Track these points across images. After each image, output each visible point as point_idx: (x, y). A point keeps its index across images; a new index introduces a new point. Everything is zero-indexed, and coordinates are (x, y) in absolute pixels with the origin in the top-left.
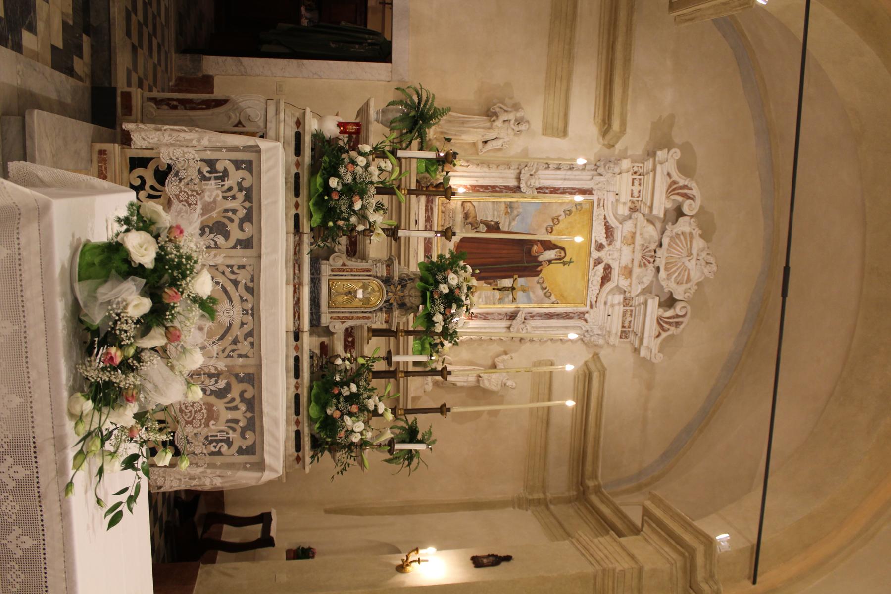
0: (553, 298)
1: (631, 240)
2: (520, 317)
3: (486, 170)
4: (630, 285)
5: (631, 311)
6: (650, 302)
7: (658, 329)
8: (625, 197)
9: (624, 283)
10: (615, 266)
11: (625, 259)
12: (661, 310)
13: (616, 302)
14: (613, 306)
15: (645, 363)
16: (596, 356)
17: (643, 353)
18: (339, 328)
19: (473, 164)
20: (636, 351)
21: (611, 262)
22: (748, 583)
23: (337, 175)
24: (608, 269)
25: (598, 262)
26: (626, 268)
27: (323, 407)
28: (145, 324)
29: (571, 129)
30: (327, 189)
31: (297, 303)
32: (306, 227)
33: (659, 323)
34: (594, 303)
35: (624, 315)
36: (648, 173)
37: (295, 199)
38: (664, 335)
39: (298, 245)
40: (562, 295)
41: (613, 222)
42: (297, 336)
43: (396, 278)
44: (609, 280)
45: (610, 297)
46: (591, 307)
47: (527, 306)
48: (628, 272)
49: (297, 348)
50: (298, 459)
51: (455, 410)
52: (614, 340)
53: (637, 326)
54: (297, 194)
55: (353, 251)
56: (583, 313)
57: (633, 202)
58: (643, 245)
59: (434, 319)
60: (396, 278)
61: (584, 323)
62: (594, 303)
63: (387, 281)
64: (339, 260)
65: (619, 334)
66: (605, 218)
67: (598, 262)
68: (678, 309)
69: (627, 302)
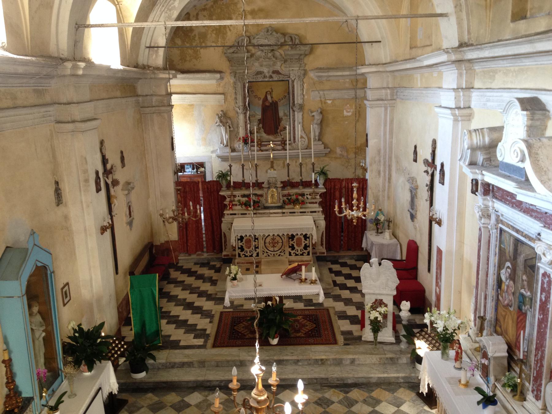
21: (271, 72)
25: (271, 77)
31: (275, 213)
39: (259, 213)
42: (284, 213)
44: (278, 71)
56: (292, 80)
63: (269, 188)
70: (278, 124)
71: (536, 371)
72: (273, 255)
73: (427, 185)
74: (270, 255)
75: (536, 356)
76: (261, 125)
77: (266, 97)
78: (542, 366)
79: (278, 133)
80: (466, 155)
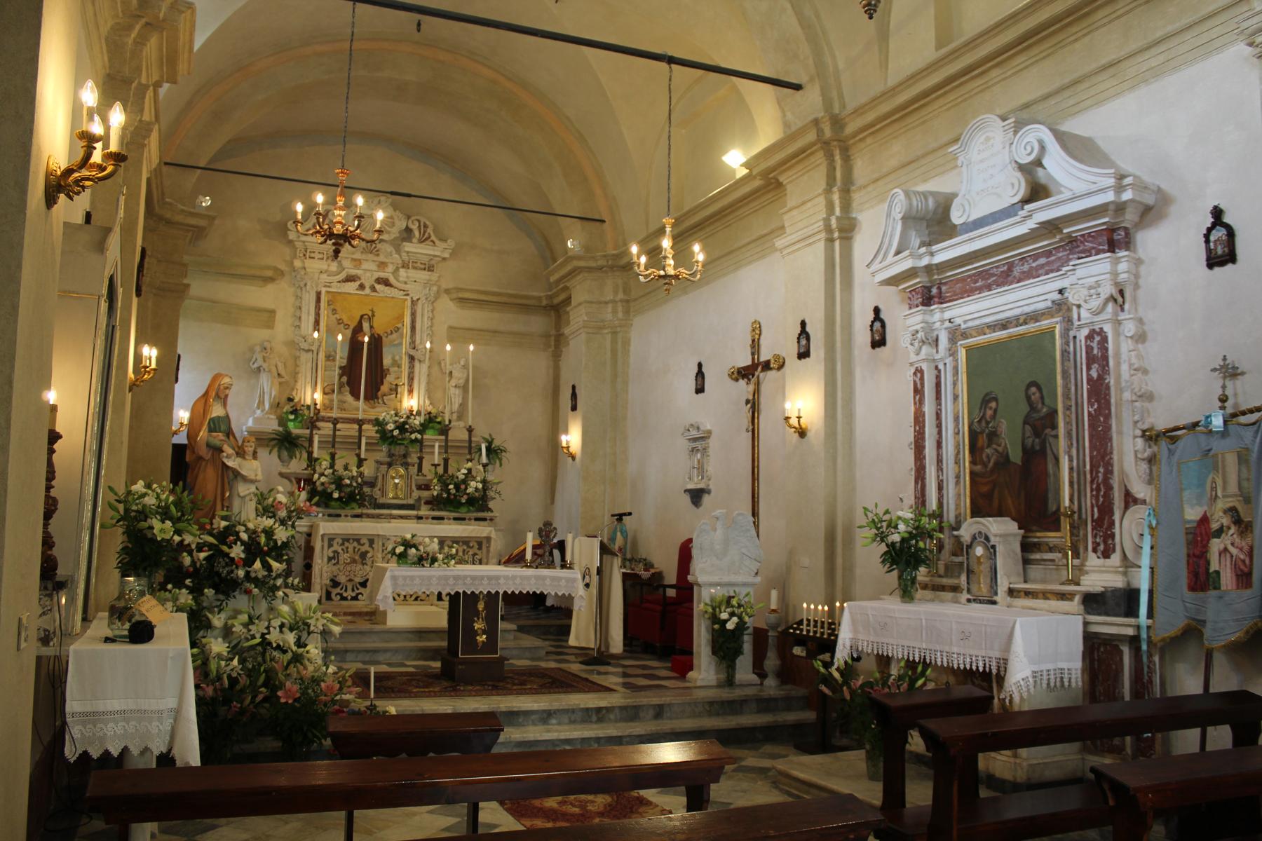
0: (400, 325)
1: (357, 263)
2: (412, 352)
3: (300, 375)
4: (392, 263)
5: (413, 262)
6: (407, 249)
7: (427, 242)
8: (323, 265)
9: (390, 268)
10: (376, 275)
11: (373, 267)
12: (415, 240)
13: (405, 274)
14: (407, 277)
15: (454, 253)
16: (447, 291)
17: (446, 255)
18: (416, 494)
19: (295, 385)
20: (444, 259)
21: (374, 278)
22: (606, 225)
23: (331, 493)
24: (379, 281)
25: (373, 289)
26: (379, 266)
27: (460, 504)
28: (417, 549)
29: (270, 306)
30: (340, 499)
31: (402, 517)
32: (359, 511)
33: (424, 241)
34: (405, 293)
35: (415, 268)
36: (305, 246)
37: (343, 517)
38: (433, 238)
39: (368, 516)
40: (398, 318)
41: (342, 276)
42: (420, 518)
43: (388, 460)
44: (387, 280)
45: (401, 279)
46: (408, 295)
47: (404, 346)
48: (382, 265)
49: (427, 518)
50: (491, 520)
51: (470, 423)
52: (434, 276)
53: (425, 259)
54: (339, 516)
55: (372, 485)
56: (412, 301)
57: (328, 258)
58: (362, 252)
59: (413, 438)
60: (388, 460)
61: (420, 301)
62: (405, 293)
63: (390, 465)
64: (377, 493)
65: (430, 273)
66: (339, 282)
67: (373, 289)
68: (414, 227)
69: (405, 266)
70: (379, 381)
71: (1098, 506)
72: (402, 598)
73: (747, 402)
74: (397, 597)
75: (1092, 482)
76: (345, 379)
77: (360, 323)
78: (1109, 488)
79: (378, 398)
80: (890, 241)
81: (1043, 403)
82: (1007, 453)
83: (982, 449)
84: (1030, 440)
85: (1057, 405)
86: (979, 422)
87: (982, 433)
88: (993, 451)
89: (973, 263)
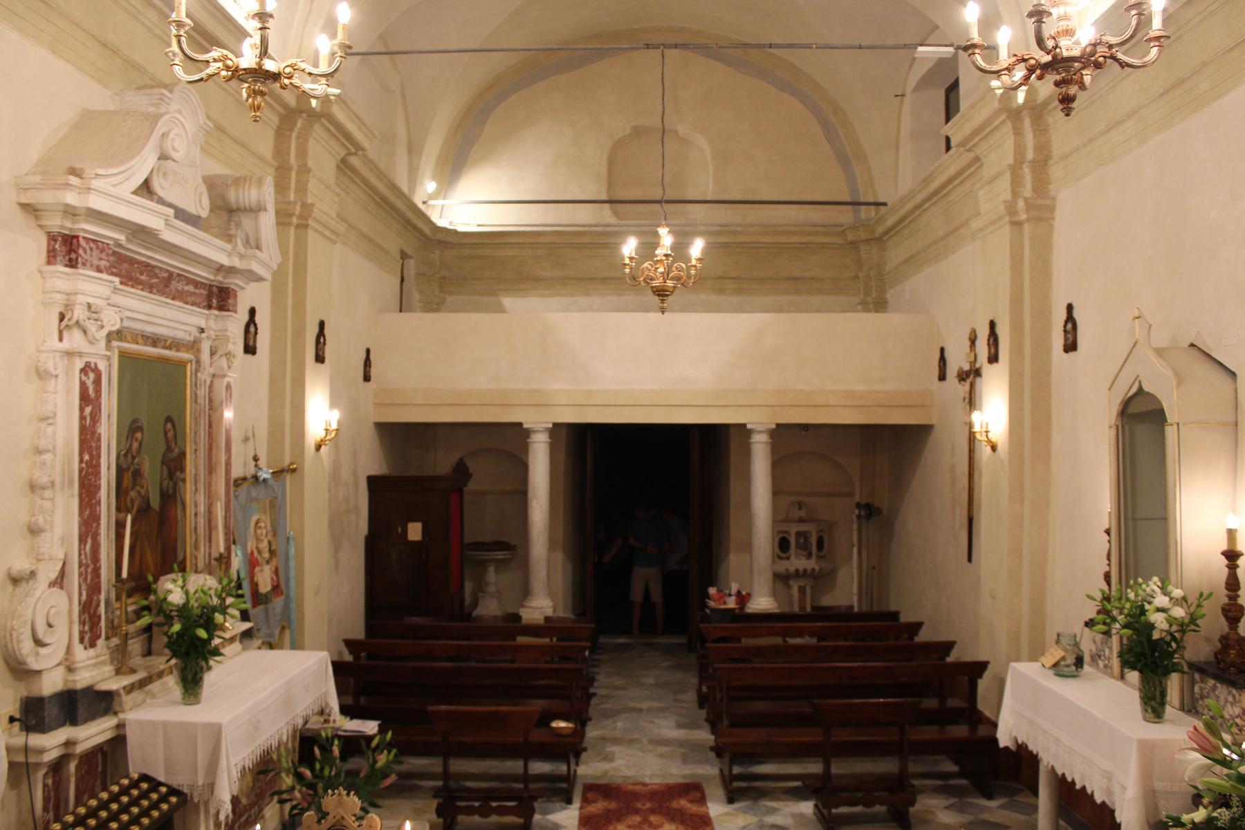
81: (176, 443)
82: (148, 497)
83: (127, 492)
84: (166, 482)
85: (185, 447)
86: (126, 455)
87: (128, 469)
88: (137, 494)
89: (156, 252)
